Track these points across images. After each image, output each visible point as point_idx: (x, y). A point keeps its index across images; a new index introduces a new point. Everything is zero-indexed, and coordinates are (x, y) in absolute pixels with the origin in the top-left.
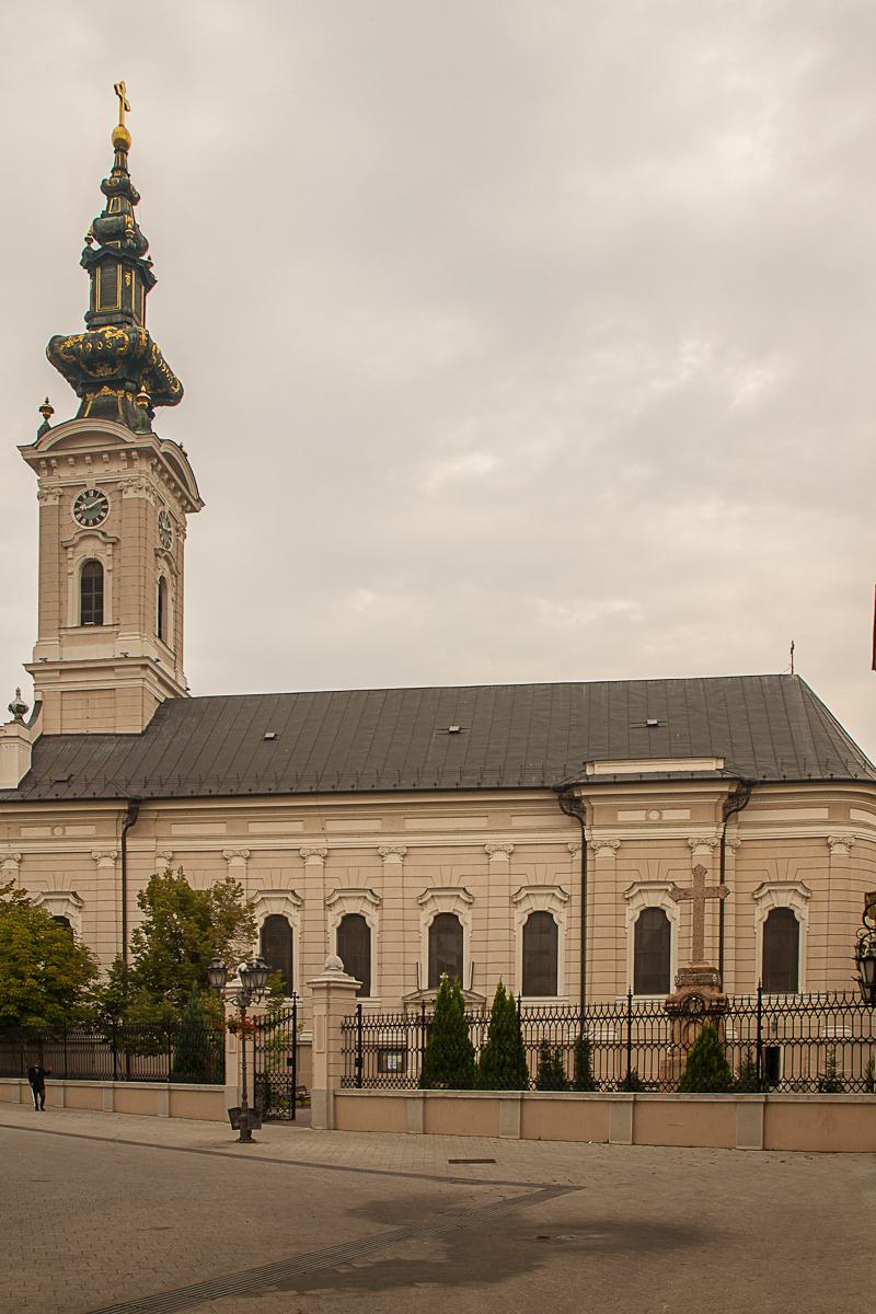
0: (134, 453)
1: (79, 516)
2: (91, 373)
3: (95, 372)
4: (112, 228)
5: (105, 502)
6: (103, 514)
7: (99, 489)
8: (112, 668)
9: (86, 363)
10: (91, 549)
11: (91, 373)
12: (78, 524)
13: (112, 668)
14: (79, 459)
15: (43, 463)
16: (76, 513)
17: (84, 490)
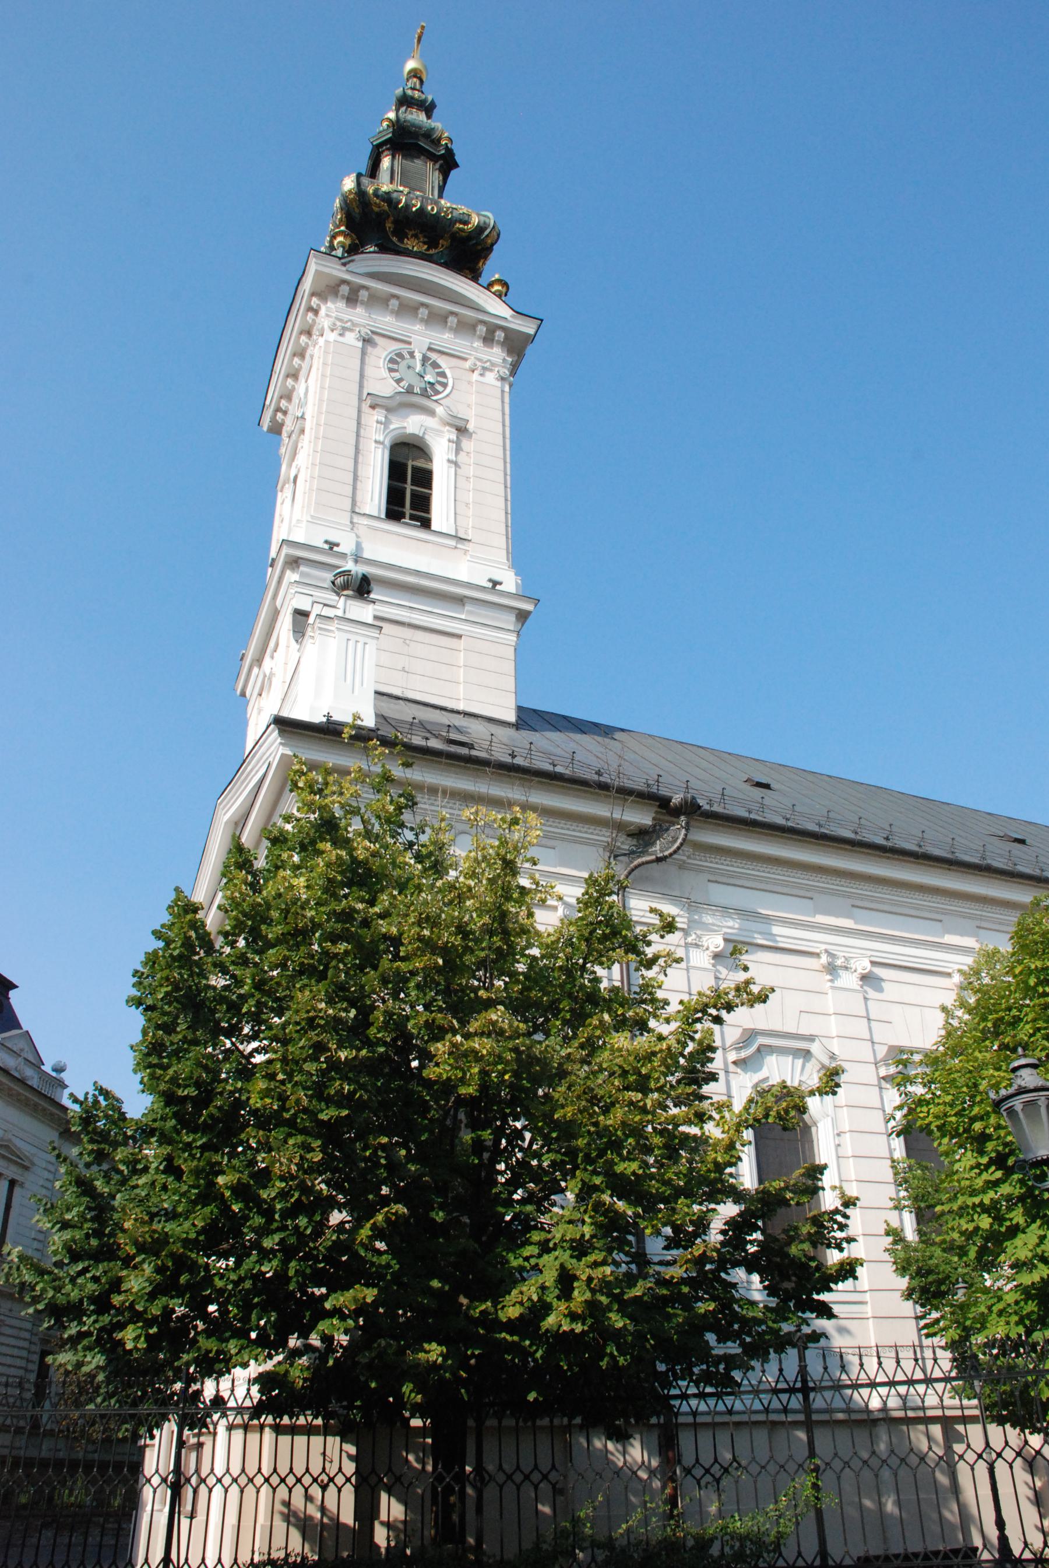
0: (500, 335)
1: (397, 375)
2: (395, 239)
3: (401, 241)
4: (420, 128)
5: (443, 375)
6: (439, 388)
7: (433, 356)
8: (460, 601)
9: (396, 222)
10: (413, 424)
11: (395, 239)
12: (395, 384)
13: (460, 601)
14: (407, 310)
15: (345, 289)
16: (391, 370)
17: (407, 346)
